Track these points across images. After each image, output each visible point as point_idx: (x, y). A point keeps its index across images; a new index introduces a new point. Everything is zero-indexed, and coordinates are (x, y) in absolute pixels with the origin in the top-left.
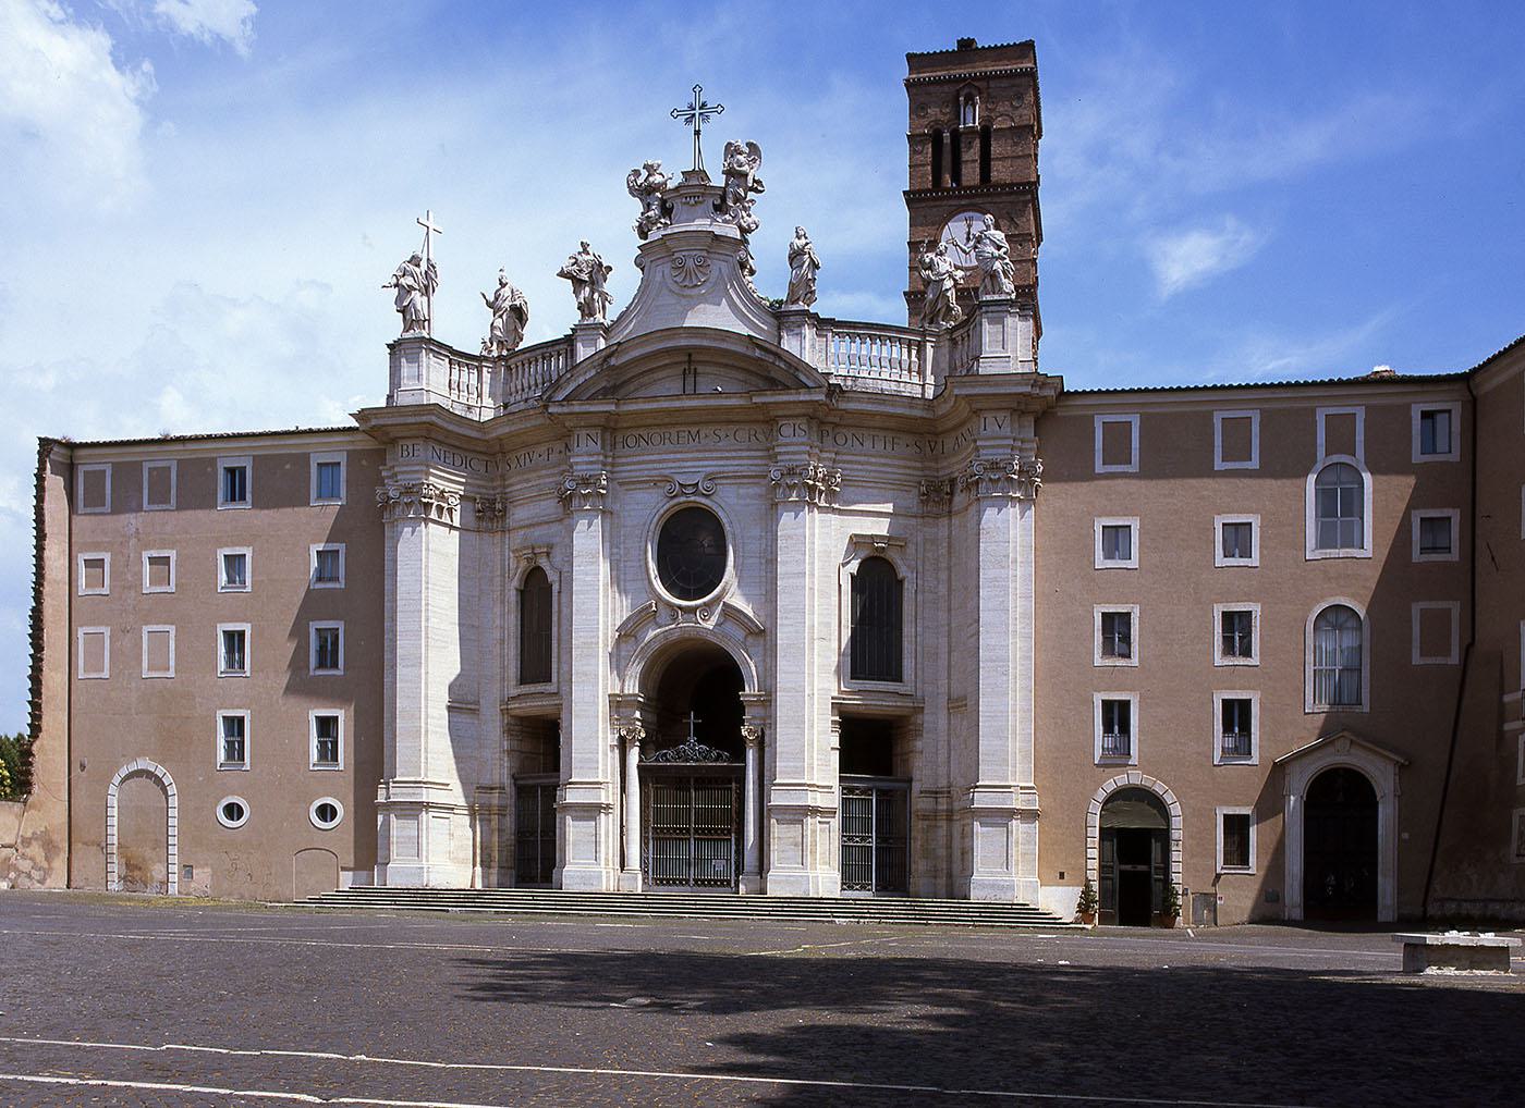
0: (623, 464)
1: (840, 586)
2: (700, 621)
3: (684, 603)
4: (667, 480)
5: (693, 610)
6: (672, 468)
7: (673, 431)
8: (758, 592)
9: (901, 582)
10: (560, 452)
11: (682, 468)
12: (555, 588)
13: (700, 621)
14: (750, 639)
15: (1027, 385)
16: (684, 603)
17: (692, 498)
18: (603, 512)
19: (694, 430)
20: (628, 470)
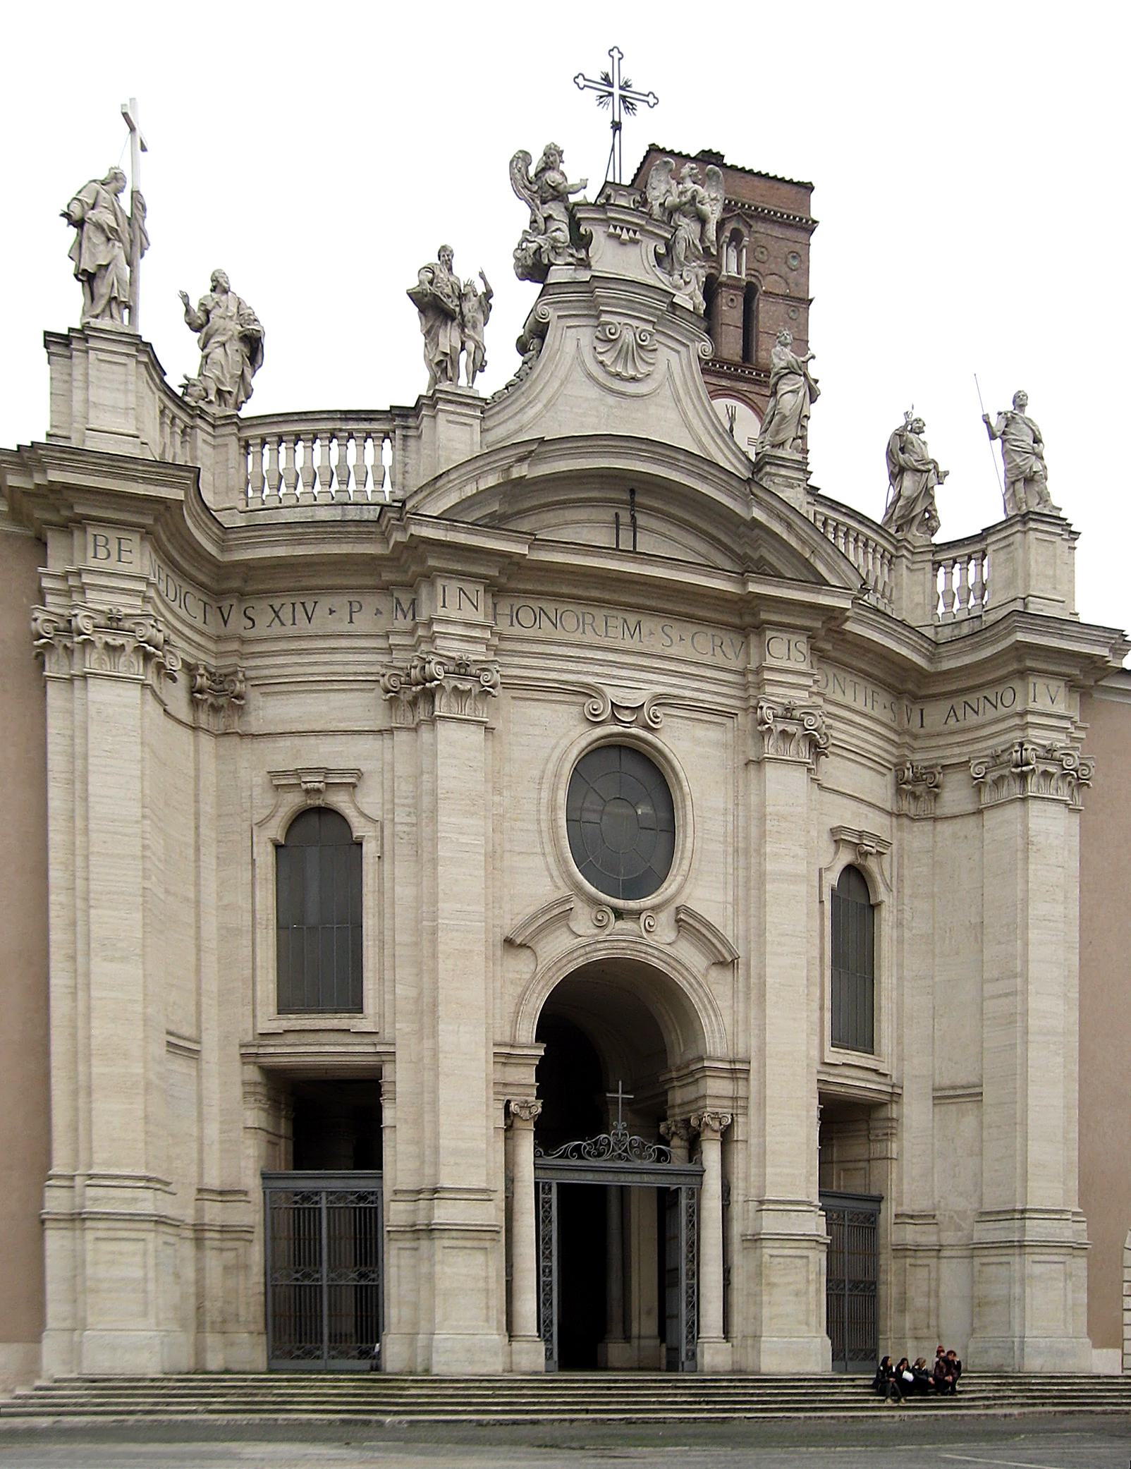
0: (514, 653)
1: (821, 902)
2: (645, 934)
3: (620, 903)
4: (588, 692)
5: (636, 914)
6: (597, 674)
7: (600, 614)
8: (720, 898)
9: (873, 908)
10: (378, 612)
11: (614, 677)
12: (370, 849)
13: (645, 934)
14: (714, 973)
15: (1104, 644)
16: (620, 903)
17: (634, 731)
18: (489, 730)
19: (632, 619)
20: (518, 666)
